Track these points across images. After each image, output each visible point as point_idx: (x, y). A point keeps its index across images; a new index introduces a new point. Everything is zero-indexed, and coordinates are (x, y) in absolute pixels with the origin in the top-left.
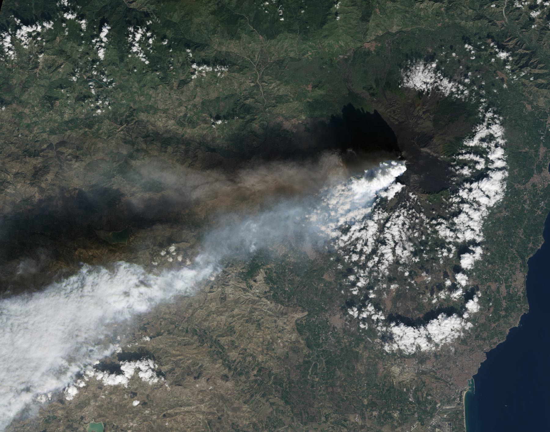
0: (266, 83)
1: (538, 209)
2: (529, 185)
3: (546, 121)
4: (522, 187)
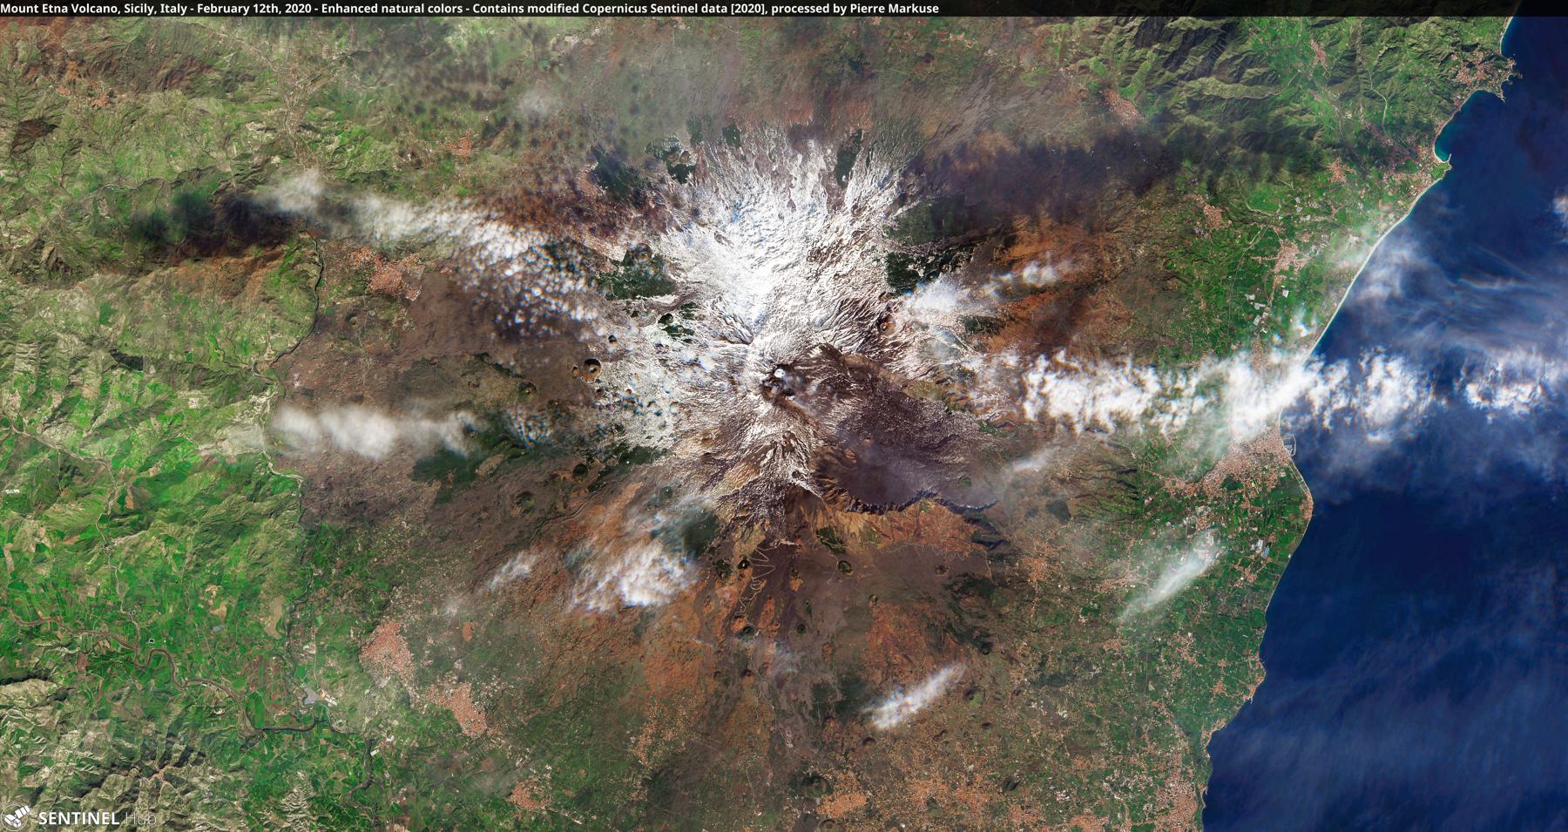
0: (316, 131)
1: (1244, 564)
3: (1273, 264)
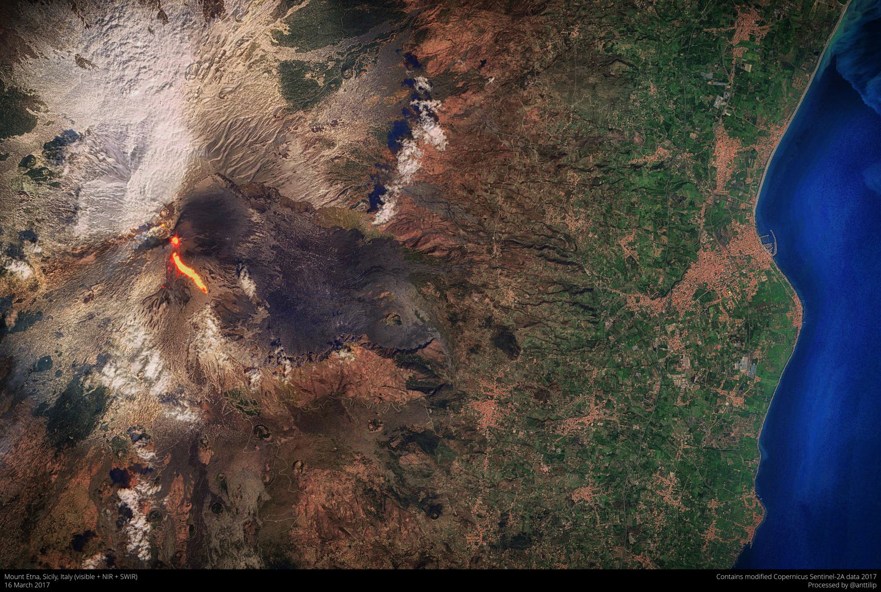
1: (729, 386)
2: (683, 297)
4: (657, 306)
